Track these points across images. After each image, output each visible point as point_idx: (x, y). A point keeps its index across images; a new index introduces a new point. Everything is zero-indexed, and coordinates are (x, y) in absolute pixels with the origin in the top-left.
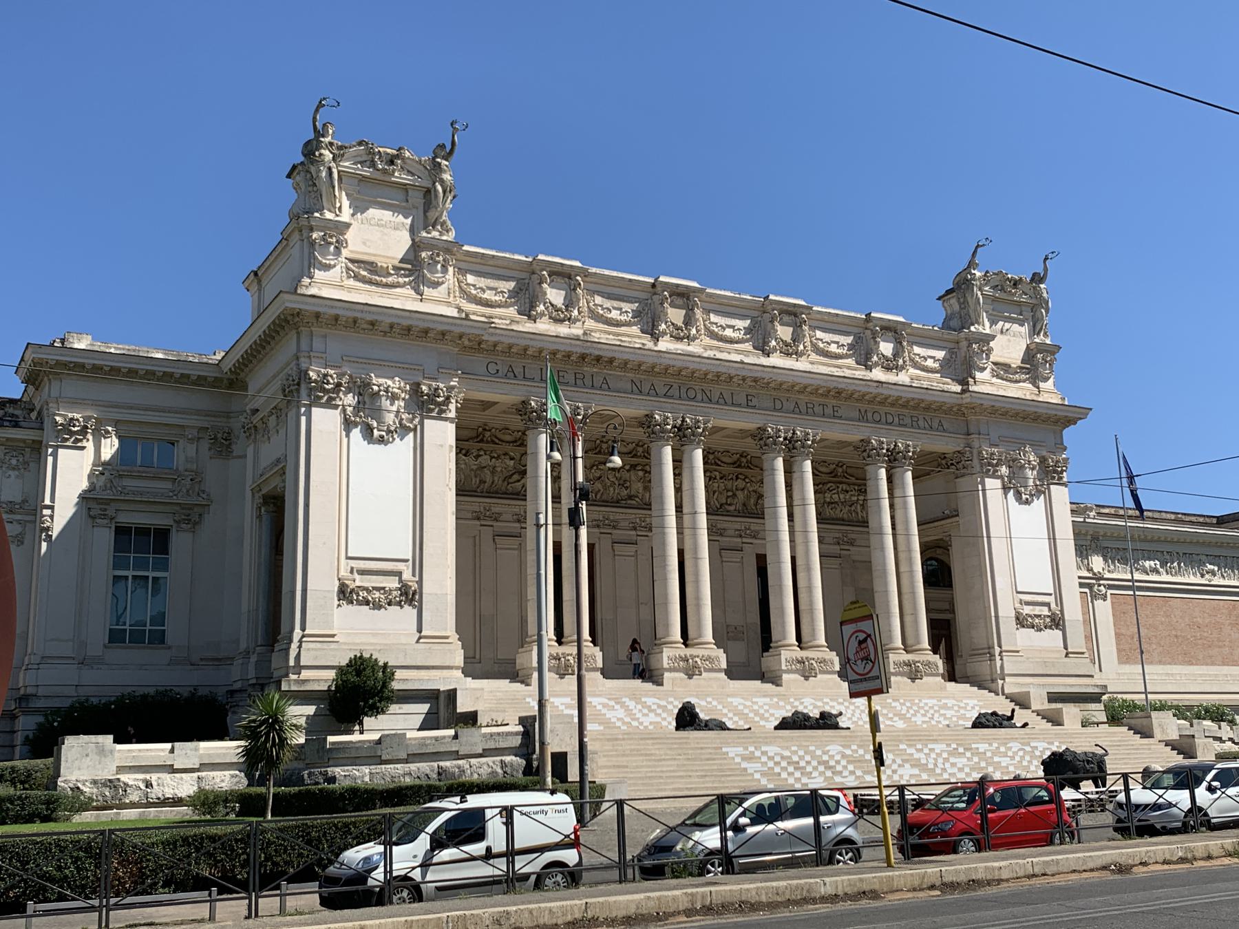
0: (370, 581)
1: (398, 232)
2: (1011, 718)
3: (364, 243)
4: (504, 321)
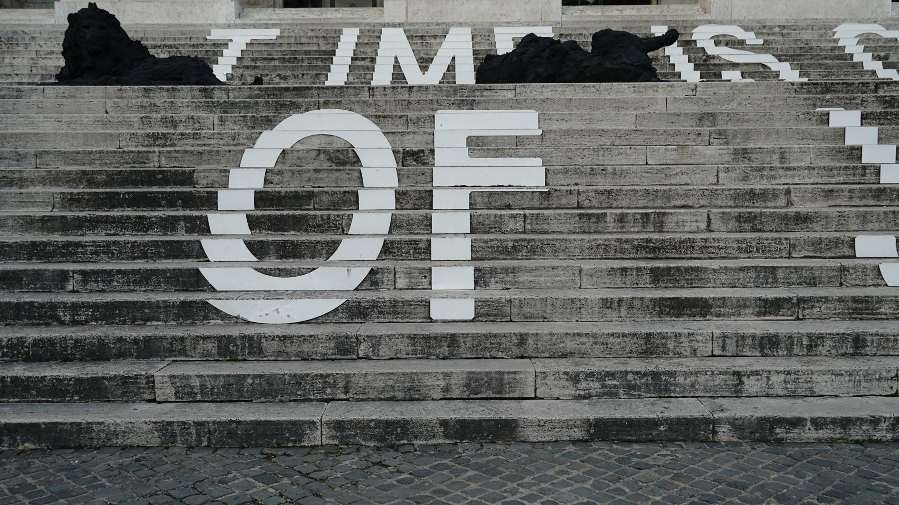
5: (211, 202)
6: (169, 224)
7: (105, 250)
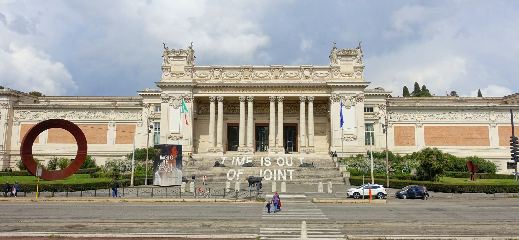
0: (173, 135)
1: (181, 66)
2: (313, 165)
3: (174, 70)
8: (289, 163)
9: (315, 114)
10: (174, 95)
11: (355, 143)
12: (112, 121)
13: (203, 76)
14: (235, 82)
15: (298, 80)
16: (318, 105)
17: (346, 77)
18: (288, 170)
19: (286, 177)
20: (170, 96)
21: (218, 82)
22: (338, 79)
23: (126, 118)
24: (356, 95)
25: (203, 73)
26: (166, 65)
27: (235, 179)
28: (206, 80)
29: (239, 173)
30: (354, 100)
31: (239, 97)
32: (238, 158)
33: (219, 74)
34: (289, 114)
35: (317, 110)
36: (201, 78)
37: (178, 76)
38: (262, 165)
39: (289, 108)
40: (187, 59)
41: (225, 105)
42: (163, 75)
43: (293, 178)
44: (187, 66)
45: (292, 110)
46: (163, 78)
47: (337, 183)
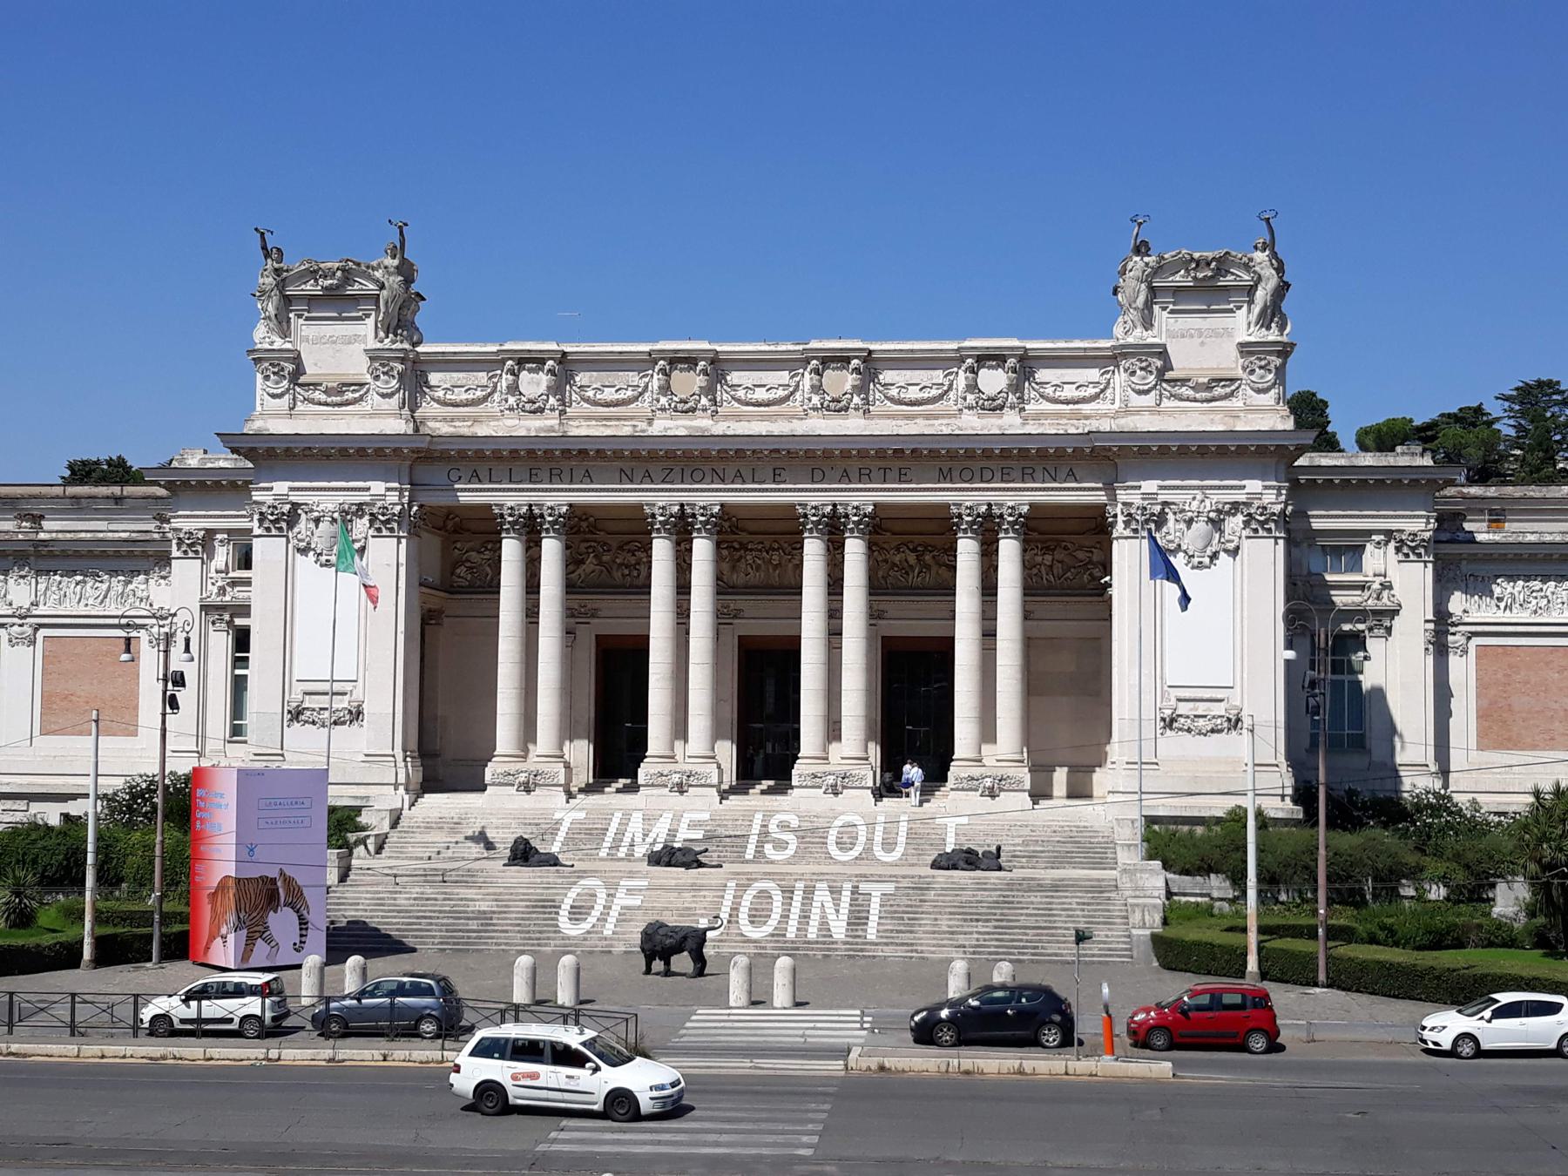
2: (999, 856)
4: (465, 423)
5: (560, 907)
6: (550, 913)
7: (538, 919)
8: (889, 845)
9: (1031, 588)
10: (316, 499)
11: (1237, 745)
12: (22, 617)
13: (464, 396)
14: (626, 430)
15: (950, 416)
16: (1059, 541)
17: (1195, 400)
18: (863, 887)
19: (845, 924)
20: (293, 504)
21: (541, 429)
22: (1156, 410)
23: (91, 601)
24: (1242, 498)
25: (464, 381)
26: (272, 343)
27: (596, 932)
28: (476, 420)
29: (621, 900)
30: (1235, 523)
31: (647, 510)
32: (637, 817)
33: (543, 389)
34: (911, 588)
35: (1058, 569)
36: (451, 409)
37: (337, 399)
38: (750, 853)
39: (912, 558)
40: (378, 309)
41: (587, 541)
42: (259, 392)
43: (881, 928)
44: (379, 345)
45: (928, 567)
46: (259, 408)
47: (1093, 956)
